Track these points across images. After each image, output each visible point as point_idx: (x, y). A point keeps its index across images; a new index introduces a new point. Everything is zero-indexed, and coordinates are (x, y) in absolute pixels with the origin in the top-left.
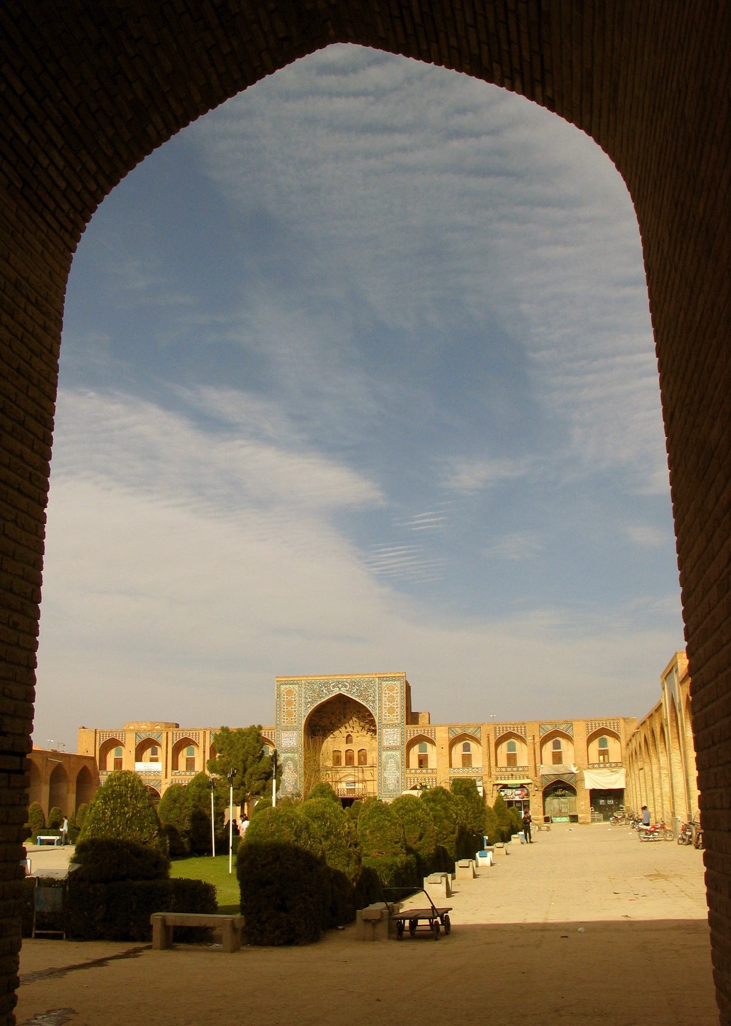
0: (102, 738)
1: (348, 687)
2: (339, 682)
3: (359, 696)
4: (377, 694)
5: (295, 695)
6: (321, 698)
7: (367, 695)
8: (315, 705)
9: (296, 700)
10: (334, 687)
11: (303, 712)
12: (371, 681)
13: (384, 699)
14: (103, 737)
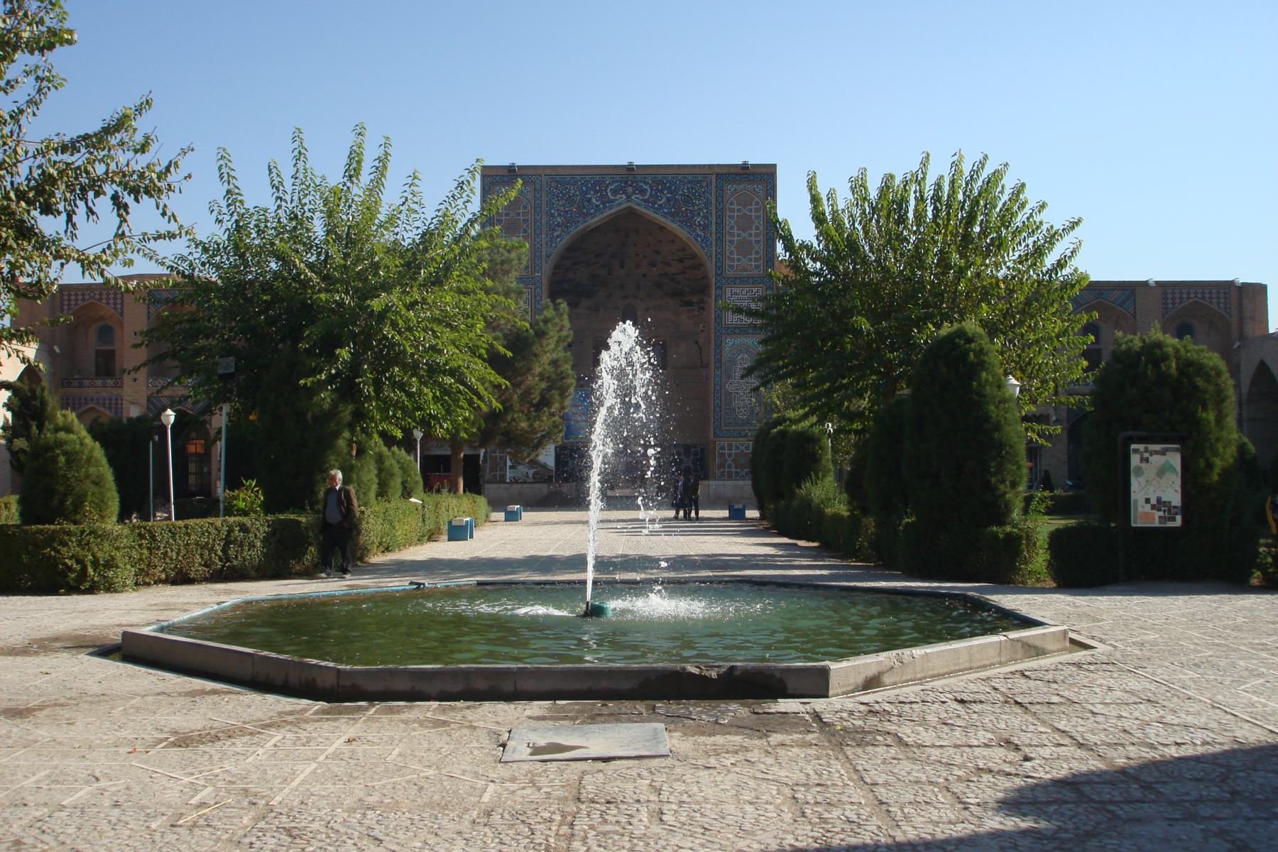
0: (66, 303)
1: (648, 193)
2: (626, 182)
3: (673, 215)
4: (714, 212)
5: (525, 207)
6: (585, 215)
7: (691, 212)
8: (573, 231)
9: (527, 220)
10: (615, 192)
11: (544, 246)
12: (699, 182)
13: (729, 223)
14: (69, 300)
